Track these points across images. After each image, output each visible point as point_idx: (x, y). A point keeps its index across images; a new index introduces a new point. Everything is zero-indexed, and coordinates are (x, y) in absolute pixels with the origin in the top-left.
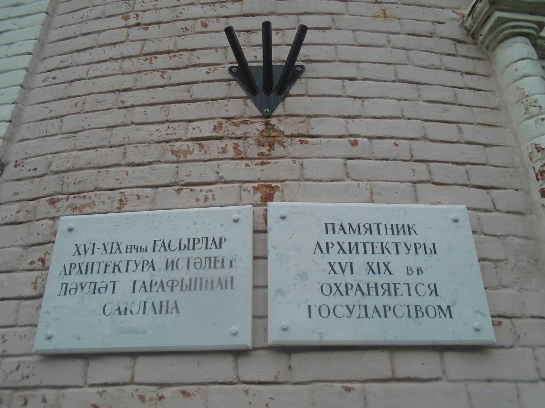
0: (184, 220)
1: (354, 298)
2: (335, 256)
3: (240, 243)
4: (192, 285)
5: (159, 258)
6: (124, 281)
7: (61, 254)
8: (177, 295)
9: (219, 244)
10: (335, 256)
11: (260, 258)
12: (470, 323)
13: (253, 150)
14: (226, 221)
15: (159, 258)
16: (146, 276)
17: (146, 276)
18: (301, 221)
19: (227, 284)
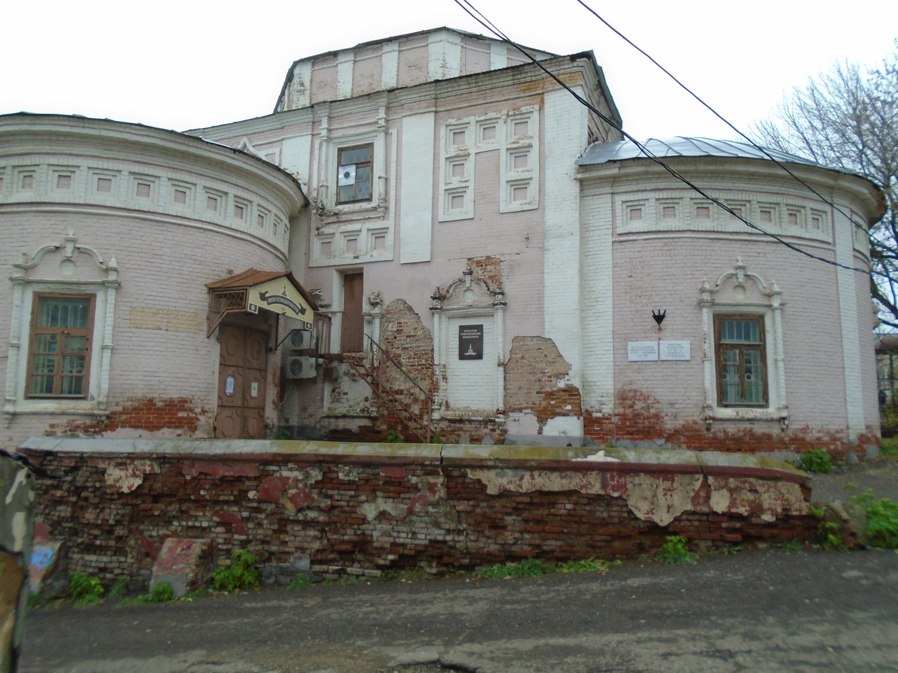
0: (648, 343)
3: (656, 347)
7: (629, 348)
12: (688, 357)
14: (654, 344)
18: (664, 344)
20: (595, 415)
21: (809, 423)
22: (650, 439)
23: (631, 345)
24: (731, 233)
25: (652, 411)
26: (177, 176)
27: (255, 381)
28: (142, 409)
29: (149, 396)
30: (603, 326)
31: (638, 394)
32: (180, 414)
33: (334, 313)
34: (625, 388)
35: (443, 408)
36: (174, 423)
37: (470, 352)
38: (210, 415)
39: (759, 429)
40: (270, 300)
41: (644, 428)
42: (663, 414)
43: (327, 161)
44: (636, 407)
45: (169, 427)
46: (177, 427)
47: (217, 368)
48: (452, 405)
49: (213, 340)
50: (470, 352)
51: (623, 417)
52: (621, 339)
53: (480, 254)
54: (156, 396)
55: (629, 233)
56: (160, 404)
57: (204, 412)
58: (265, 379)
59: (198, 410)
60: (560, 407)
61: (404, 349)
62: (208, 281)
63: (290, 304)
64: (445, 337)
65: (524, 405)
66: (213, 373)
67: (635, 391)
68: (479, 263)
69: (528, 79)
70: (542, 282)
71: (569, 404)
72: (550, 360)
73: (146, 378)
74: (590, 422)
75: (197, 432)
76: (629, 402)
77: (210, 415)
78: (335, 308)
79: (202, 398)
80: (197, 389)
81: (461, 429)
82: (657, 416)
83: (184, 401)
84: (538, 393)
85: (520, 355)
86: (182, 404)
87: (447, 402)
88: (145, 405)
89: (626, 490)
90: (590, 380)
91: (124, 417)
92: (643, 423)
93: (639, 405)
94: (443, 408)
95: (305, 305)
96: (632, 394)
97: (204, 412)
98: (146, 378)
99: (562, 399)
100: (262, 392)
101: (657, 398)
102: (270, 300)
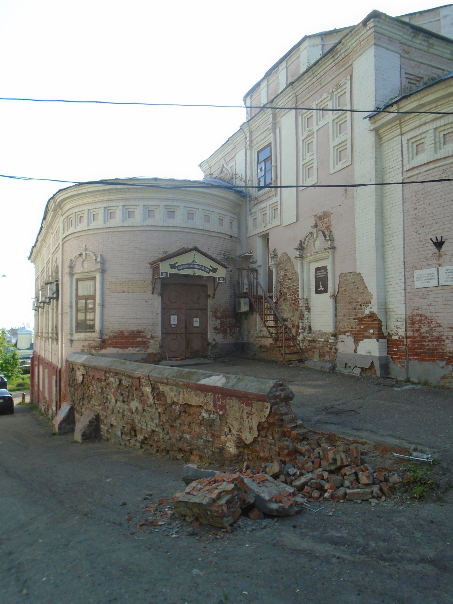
1: (450, 279)
2: (448, 274)
3: (436, 274)
4: (431, 279)
5: (427, 276)
6: (423, 279)
8: (429, 281)
9: (433, 273)
10: (448, 274)
11: (438, 275)
13: (437, 258)
14: (434, 271)
15: (427, 276)
16: (425, 278)
17: (425, 278)
18: (442, 270)
19: (434, 279)
20: (395, 337)
22: (433, 361)
23: (417, 273)
25: (435, 334)
27: (197, 317)
28: (117, 337)
29: (121, 330)
30: (395, 260)
31: (423, 318)
32: (138, 339)
33: (260, 266)
34: (414, 313)
35: (306, 331)
36: (134, 344)
37: (321, 289)
38: (156, 339)
40: (179, 268)
41: (429, 349)
42: (444, 338)
43: (251, 163)
44: (422, 331)
45: (132, 347)
46: (136, 347)
47: (159, 311)
48: (314, 329)
49: (156, 296)
50: (321, 289)
51: (413, 338)
52: (408, 268)
53: (320, 212)
54: (124, 329)
55: (414, 168)
56: (126, 334)
57: (152, 337)
58: (206, 314)
59: (149, 337)
60: (366, 331)
61: (288, 288)
62: (150, 261)
63: (201, 267)
64: (306, 277)
65: (347, 329)
66: (157, 314)
67: (421, 315)
68: (320, 218)
69: (343, 56)
70: (354, 227)
71: (372, 328)
72: (361, 291)
73: (119, 320)
74: (391, 343)
75: (149, 349)
76: (417, 326)
77: (156, 339)
78: (259, 263)
79: (151, 329)
80: (147, 325)
81: (315, 347)
82: (438, 339)
83: (140, 332)
84: (355, 319)
85: (344, 289)
86: (139, 333)
87: (310, 327)
88: (119, 335)
89: (226, 410)
90: (390, 306)
91: (110, 342)
92: (428, 345)
93: (424, 329)
94: (306, 331)
95: (215, 265)
96: (418, 318)
97: (152, 337)
98: (119, 320)
99: (372, 325)
100: (204, 323)
101: (439, 322)
102: (179, 268)
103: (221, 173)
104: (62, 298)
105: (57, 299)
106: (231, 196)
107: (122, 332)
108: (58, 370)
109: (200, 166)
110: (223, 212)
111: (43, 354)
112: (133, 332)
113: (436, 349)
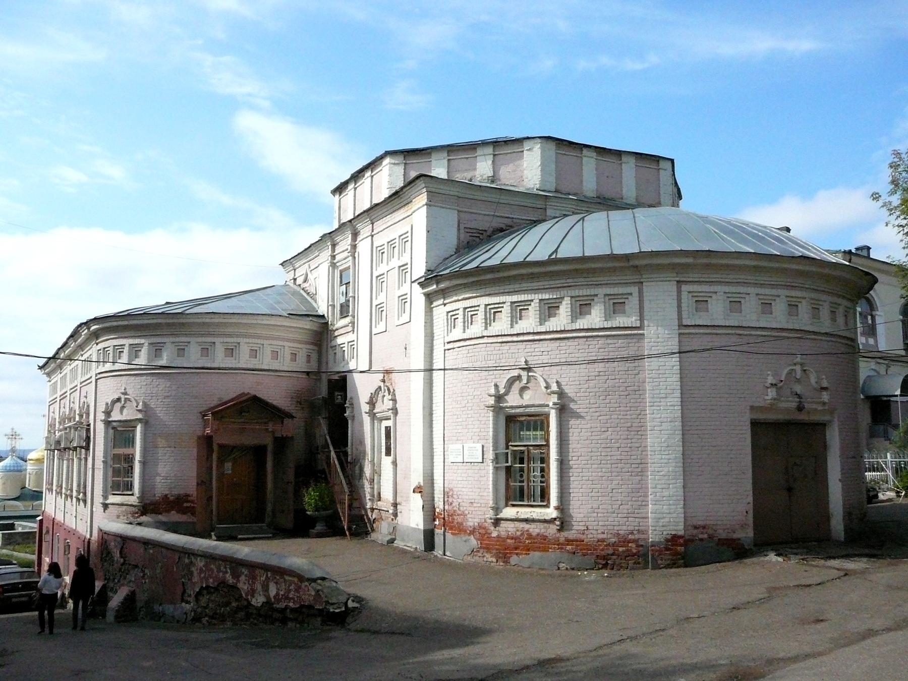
21: (588, 524)
24: (518, 335)
26: (177, 340)
32: (185, 505)
39: (535, 529)
103: (305, 281)
104: (94, 449)
105: (87, 448)
106: (307, 324)
107: (166, 495)
108: (86, 541)
109: (281, 264)
110: (296, 345)
111: (59, 517)
112: (179, 495)
113: (462, 524)
